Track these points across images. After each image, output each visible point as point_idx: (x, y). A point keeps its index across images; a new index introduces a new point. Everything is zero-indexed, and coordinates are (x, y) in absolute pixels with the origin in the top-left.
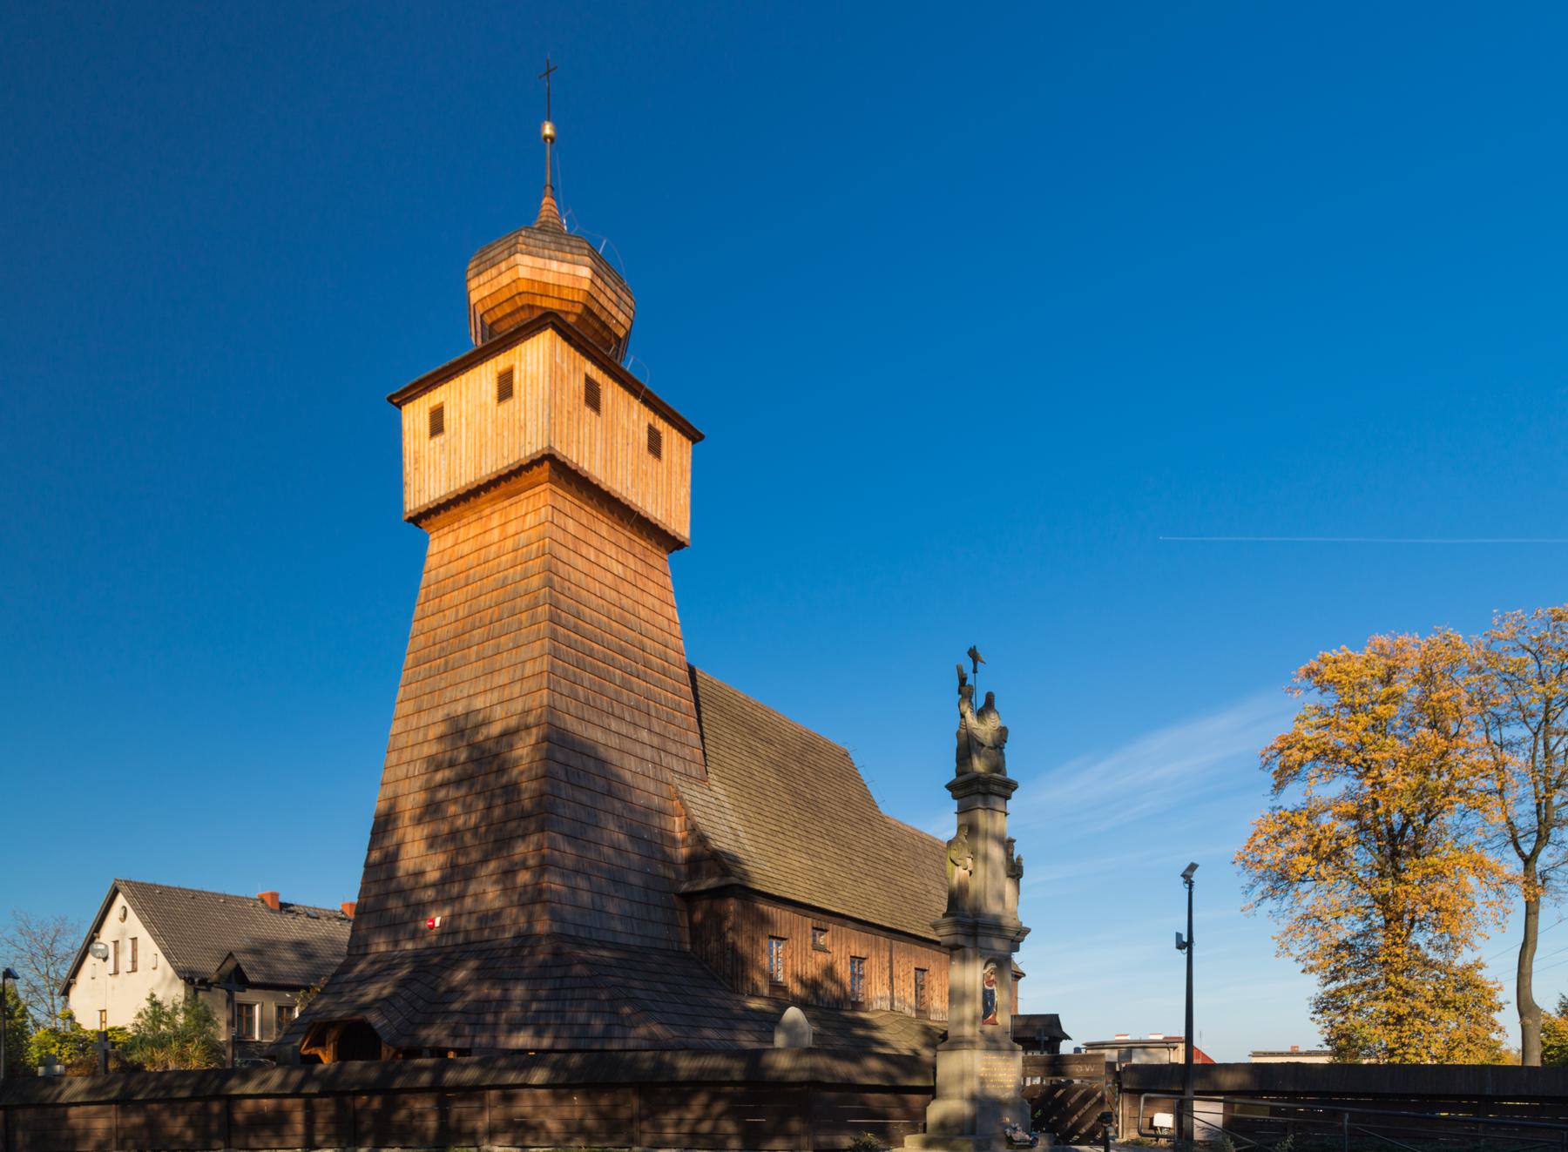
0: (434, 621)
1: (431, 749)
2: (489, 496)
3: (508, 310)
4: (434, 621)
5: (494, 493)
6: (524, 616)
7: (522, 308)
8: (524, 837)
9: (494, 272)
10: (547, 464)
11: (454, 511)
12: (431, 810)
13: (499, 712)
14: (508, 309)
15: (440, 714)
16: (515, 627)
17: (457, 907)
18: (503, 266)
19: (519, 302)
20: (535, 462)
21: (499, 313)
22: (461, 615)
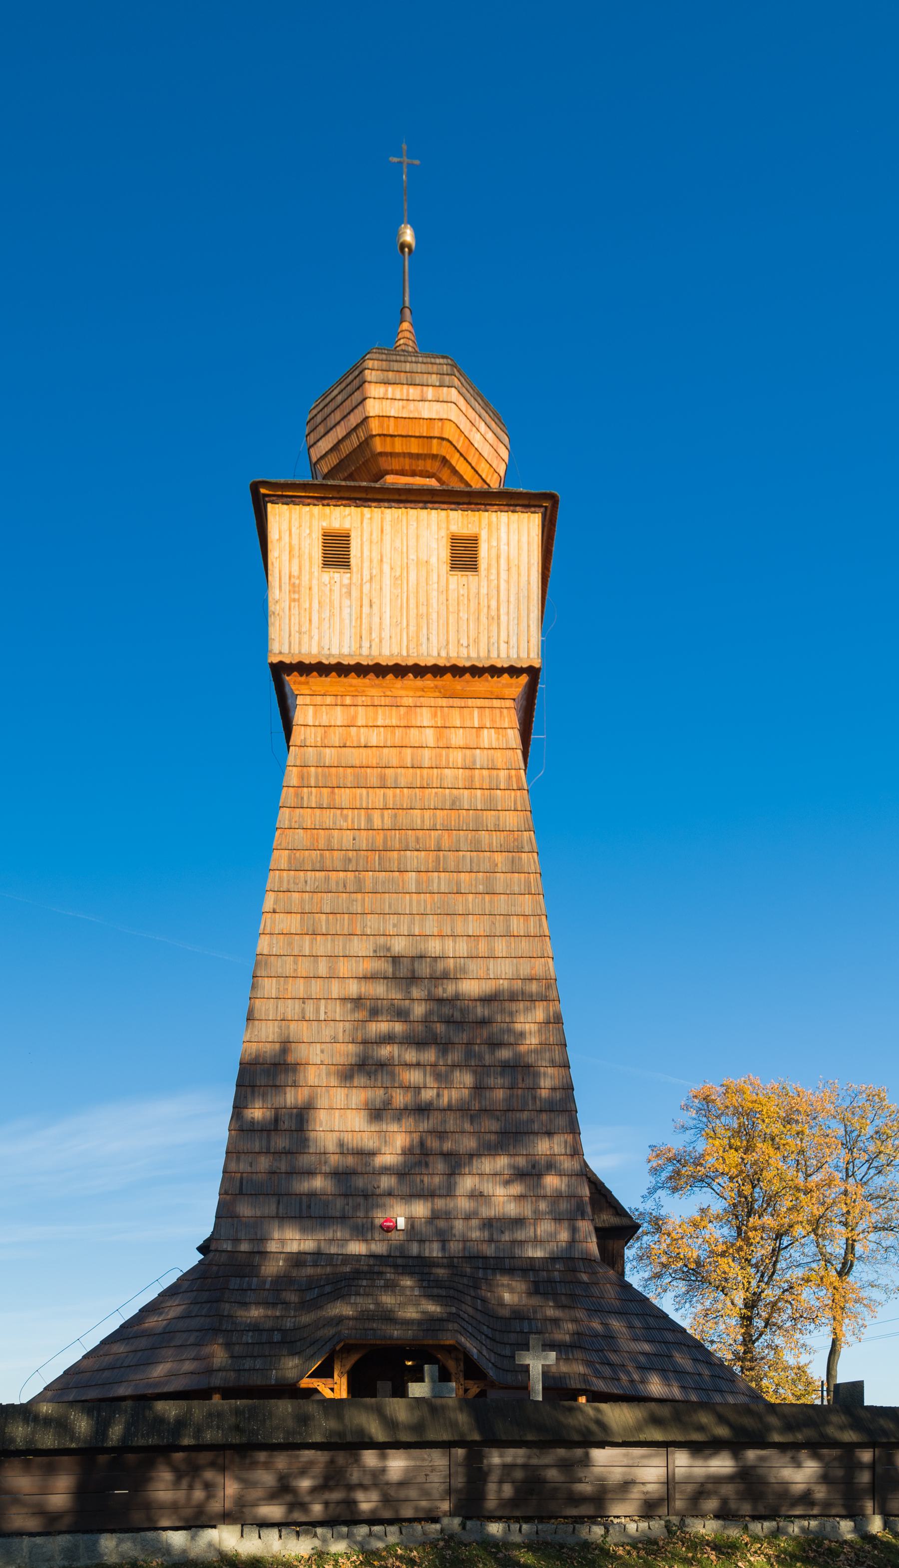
0: (328, 818)
1: (353, 989)
2: (419, 682)
3: (414, 450)
4: (328, 818)
5: (429, 681)
6: (499, 858)
7: (434, 457)
8: (549, 1134)
9: (414, 392)
10: (524, 679)
11: (353, 680)
12: (365, 1067)
13: (473, 967)
14: (414, 447)
15: (361, 947)
16: (487, 866)
17: (440, 1203)
18: (430, 393)
19: (435, 448)
20: (513, 671)
21: (399, 446)
22: (377, 823)
